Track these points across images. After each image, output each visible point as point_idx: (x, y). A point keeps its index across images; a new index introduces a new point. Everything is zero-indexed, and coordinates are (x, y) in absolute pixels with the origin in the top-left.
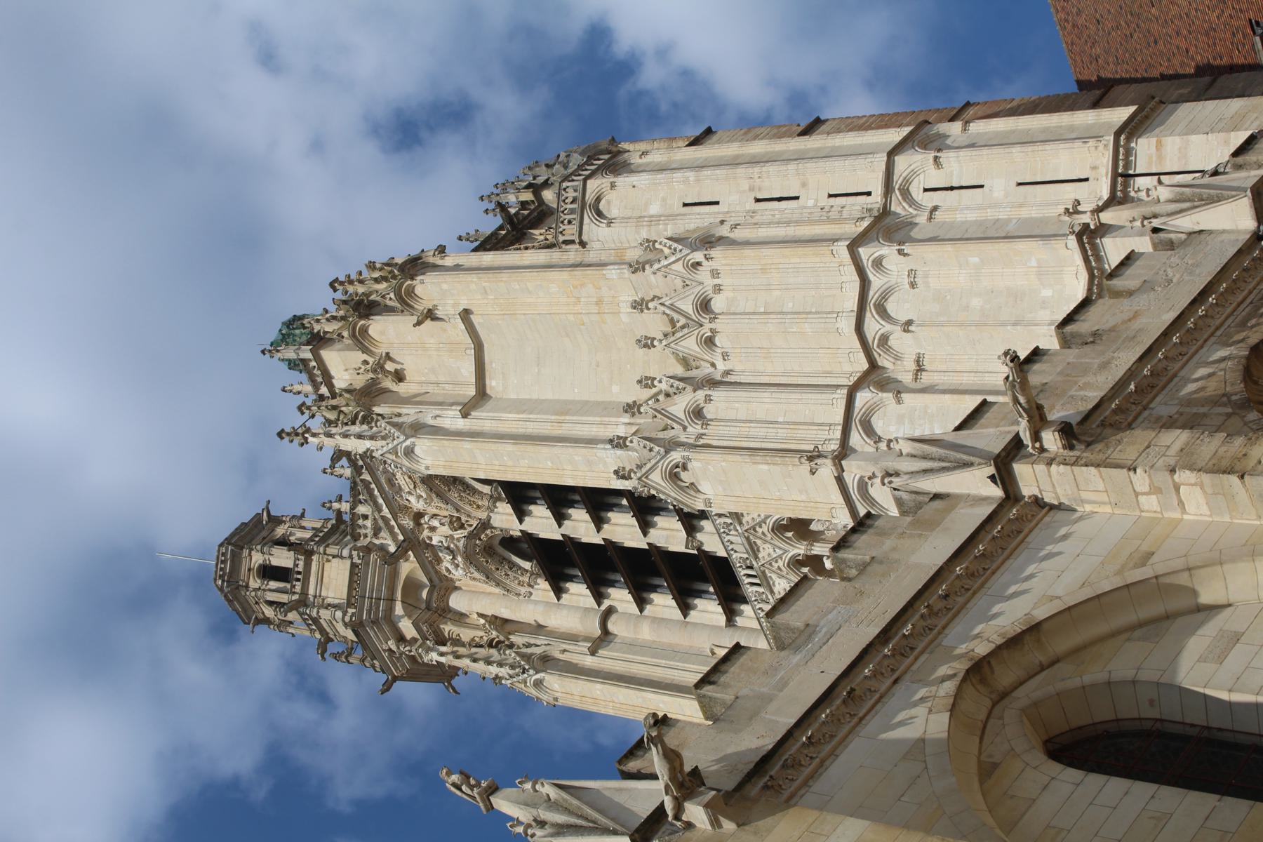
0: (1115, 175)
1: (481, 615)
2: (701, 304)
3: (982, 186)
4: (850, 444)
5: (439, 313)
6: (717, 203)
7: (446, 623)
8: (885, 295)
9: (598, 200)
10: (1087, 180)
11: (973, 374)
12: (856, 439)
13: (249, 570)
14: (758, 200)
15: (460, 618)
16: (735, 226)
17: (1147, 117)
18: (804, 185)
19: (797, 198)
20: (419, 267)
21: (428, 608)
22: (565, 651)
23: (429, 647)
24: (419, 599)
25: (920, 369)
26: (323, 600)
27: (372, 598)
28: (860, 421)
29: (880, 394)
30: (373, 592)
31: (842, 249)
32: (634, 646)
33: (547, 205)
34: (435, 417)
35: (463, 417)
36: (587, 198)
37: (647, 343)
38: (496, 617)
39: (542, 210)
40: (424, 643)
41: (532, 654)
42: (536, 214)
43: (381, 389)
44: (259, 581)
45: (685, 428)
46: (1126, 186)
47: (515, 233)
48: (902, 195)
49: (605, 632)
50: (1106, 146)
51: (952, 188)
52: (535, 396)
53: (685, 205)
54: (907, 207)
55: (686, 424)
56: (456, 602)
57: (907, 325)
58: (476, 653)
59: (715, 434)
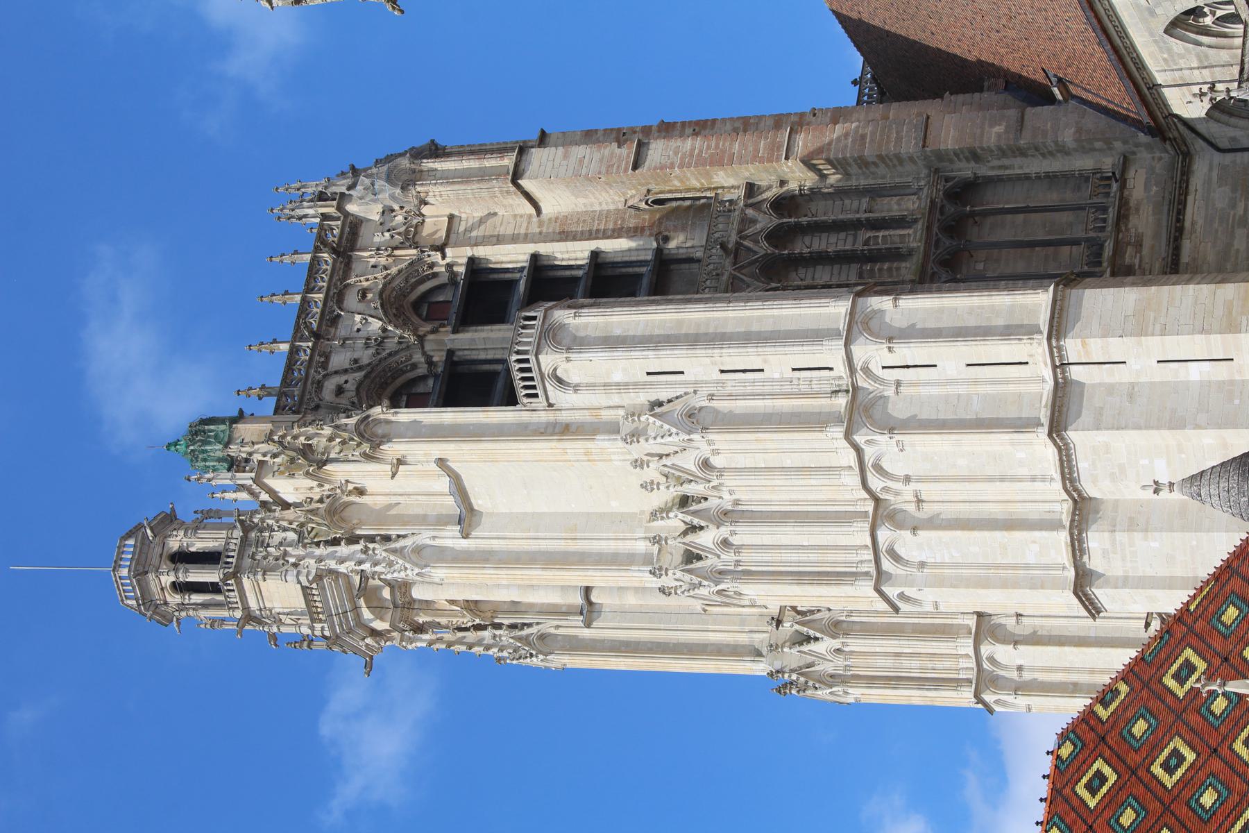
0: (1055, 367)
1: (452, 602)
2: (702, 463)
3: (935, 366)
4: (884, 568)
5: (409, 459)
6: (682, 373)
7: (417, 615)
8: (878, 459)
9: (555, 369)
10: (1027, 363)
11: (968, 504)
12: (887, 565)
13: (162, 589)
14: (722, 371)
15: (427, 605)
16: (711, 397)
17: (1061, 310)
18: (765, 361)
19: (762, 370)
20: (371, 426)
21: (395, 607)
22: (558, 627)
23: (410, 638)
24: (382, 599)
25: (919, 501)
26: (270, 610)
27: (339, 614)
28: (886, 551)
29: (898, 531)
30: (337, 609)
31: (838, 432)
32: (623, 612)
33: (353, 215)
34: (434, 537)
35: (463, 538)
36: (543, 370)
37: (648, 486)
38: (467, 601)
39: (351, 223)
40: (403, 636)
41: (528, 636)
42: (347, 229)
43: (345, 503)
44: (178, 597)
45: (719, 557)
46: (1063, 372)
47: (341, 259)
48: (864, 374)
49: (590, 603)
50: (1039, 344)
51: (908, 367)
52: (529, 510)
53: (648, 374)
54: (873, 383)
55: (719, 553)
56: (418, 593)
57: (907, 479)
58: (465, 637)
59: (750, 559)
